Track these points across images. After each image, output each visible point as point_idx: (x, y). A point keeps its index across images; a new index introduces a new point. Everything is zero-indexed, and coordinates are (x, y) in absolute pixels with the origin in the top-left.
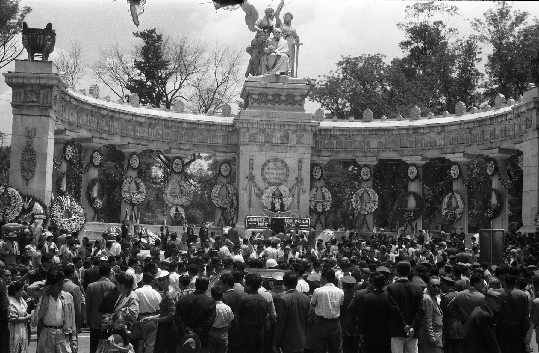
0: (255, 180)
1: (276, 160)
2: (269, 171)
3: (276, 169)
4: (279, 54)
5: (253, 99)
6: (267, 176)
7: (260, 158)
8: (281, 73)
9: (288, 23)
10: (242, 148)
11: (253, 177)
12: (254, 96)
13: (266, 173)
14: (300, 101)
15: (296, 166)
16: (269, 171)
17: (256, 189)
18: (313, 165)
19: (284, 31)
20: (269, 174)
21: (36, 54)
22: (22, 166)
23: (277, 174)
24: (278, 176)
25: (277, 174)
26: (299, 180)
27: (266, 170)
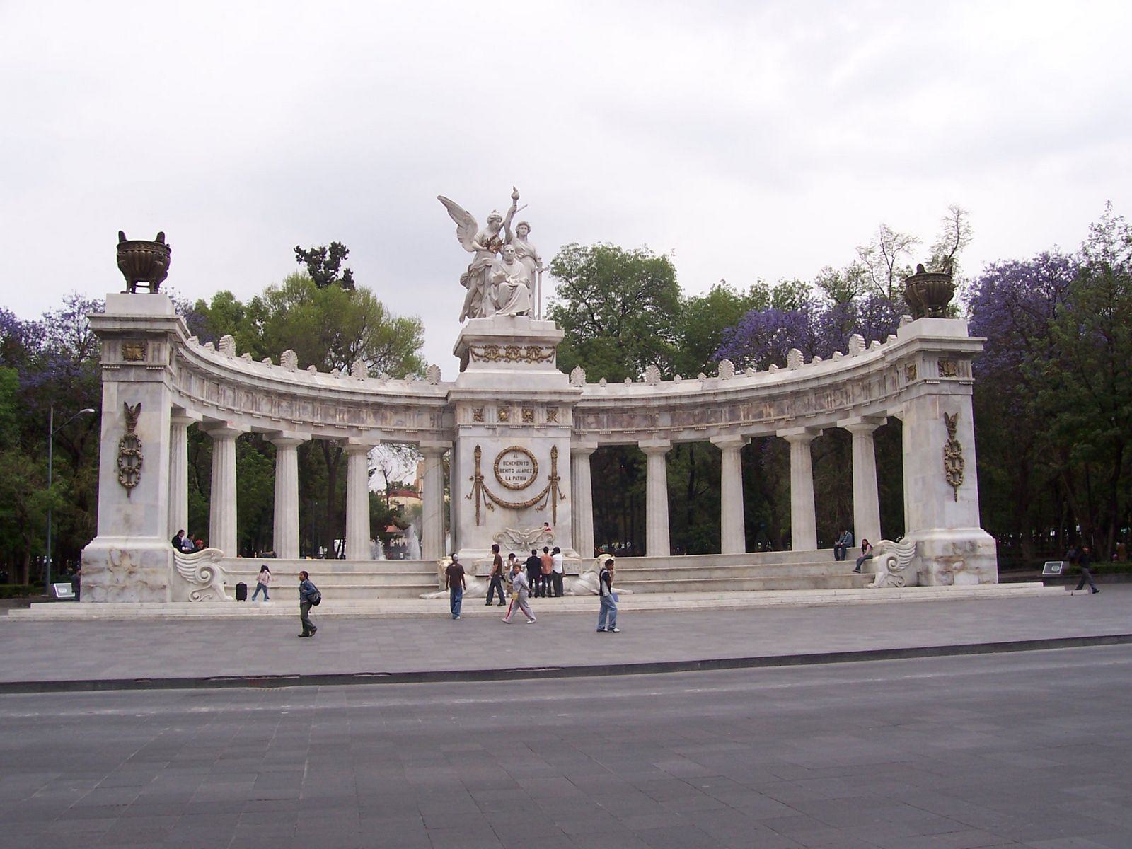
0: (484, 481)
1: (515, 450)
2: (506, 467)
4: (514, 284)
5: (477, 355)
6: (503, 476)
7: (491, 448)
8: (518, 314)
9: (522, 236)
10: (462, 433)
12: (477, 351)
13: (502, 471)
15: (548, 457)
16: (506, 467)
17: (487, 498)
18: (573, 456)
19: (518, 250)
20: (507, 471)
21: (139, 283)
22: (119, 466)
23: (518, 471)
25: (518, 471)
26: (554, 479)
27: (501, 466)
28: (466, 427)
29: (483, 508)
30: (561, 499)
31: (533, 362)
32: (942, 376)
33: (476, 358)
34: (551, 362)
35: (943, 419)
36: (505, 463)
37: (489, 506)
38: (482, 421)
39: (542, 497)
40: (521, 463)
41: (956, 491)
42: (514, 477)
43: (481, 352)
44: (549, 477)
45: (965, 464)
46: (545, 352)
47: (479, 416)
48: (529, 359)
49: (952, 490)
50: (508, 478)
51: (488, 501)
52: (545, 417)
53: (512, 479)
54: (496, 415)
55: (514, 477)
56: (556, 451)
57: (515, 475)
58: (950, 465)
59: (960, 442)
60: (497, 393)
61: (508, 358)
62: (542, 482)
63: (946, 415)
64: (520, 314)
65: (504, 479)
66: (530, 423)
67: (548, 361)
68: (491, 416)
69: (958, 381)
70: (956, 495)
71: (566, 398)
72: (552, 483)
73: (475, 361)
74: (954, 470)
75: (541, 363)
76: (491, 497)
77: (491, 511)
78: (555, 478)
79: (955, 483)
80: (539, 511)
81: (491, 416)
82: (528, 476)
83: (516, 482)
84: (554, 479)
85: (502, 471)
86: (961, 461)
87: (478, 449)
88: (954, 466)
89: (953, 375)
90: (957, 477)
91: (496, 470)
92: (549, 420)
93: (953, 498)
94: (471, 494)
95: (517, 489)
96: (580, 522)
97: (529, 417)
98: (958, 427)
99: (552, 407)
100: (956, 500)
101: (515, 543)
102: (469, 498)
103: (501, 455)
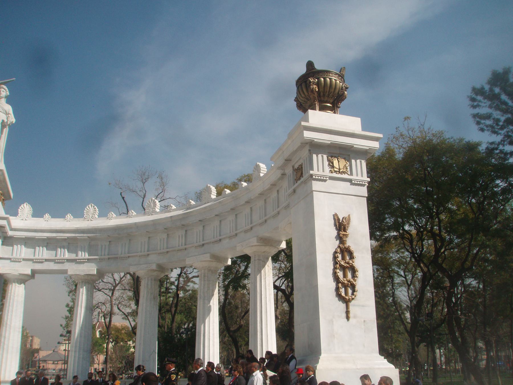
32: (332, 173)
35: (332, 222)
41: (347, 307)
45: (359, 274)
49: (343, 306)
58: (340, 274)
59: (352, 248)
63: (336, 217)
69: (350, 181)
70: (347, 312)
74: (346, 282)
79: (347, 298)
86: (354, 271)
88: (345, 276)
89: (344, 172)
90: (350, 291)
93: (344, 315)
96: (4, 343)
98: (350, 231)
100: (348, 318)
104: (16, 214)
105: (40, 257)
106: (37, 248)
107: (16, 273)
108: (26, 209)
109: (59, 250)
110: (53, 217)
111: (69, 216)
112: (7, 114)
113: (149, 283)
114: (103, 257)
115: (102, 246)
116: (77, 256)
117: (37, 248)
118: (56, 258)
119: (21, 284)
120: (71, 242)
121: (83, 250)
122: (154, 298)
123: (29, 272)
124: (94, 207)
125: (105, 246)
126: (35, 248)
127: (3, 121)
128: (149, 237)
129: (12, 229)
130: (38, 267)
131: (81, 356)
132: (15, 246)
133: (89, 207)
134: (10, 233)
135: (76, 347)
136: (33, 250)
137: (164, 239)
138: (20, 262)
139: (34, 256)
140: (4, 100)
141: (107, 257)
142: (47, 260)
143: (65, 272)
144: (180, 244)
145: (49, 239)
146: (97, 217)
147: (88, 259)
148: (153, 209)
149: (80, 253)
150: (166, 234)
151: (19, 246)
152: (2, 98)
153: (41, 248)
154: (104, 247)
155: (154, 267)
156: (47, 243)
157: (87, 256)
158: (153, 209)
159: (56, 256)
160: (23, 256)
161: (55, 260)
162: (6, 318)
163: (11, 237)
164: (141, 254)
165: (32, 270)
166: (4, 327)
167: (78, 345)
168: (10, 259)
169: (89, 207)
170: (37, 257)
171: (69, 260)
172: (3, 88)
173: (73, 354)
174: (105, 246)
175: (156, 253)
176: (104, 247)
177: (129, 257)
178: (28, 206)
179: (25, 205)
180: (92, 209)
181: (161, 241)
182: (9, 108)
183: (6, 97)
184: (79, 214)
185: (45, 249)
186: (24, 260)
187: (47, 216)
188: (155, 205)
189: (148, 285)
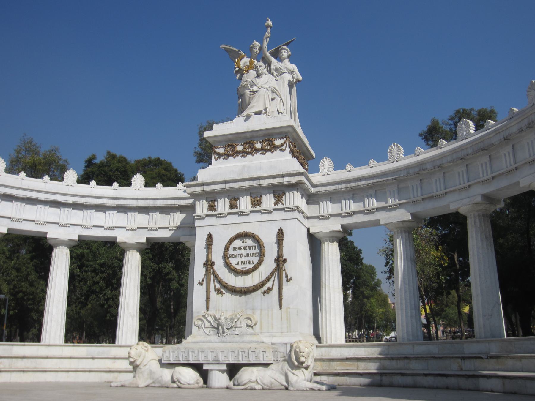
0: (215, 267)
3: (245, 248)
6: (232, 261)
8: (256, 113)
10: (197, 223)
11: (213, 264)
12: (218, 150)
13: (231, 256)
14: (282, 145)
16: (235, 252)
20: (236, 256)
23: (247, 256)
24: (249, 259)
25: (247, 256)
26: (280, 261)
27: (231, 252)
28: (202, 218)
29: (213, 294)
30: (288, 281)
31: (267, 153)
33: (217, 157)
34: (284, 151)
36: (234, 249)
37: (218, 291)
38: (215, 210)
39: (268, 279)
40: (249, 248)
42: (242, 262)
43: (221, 150)
44: (275, 259)
46: (278, 142)
47: (212, 208)
48: (264, 151)
50: (236, 263)
51: (218, 286)
52: (273, 201)
53: (240, 263)
54: (228, 204)
55: (242, 262)
56: (282, 233)
57: (244, 260)
60: (226, 182)
61: (245, 153)
62: (269, 265)
64: (258, 113)
65: (233, 264)
66: (258, 208)
67: (281, 150)
68: (223, 205)
71: (286, 180)
72: (278, 265)
73: (216, 160)
75: (275, 152)
76: (220, 282)
77: (220, 295)
78: (281, 259)
80: (265, 294)
81: (223, 205)
82: (256, 260)
83: (243, 266)
84: (280, 261)
85: (231, 256)
87: (210, 238)
91: (225, 257)
92: (276, 204)
94: (203, 281)
95: (247, 273)
97: (256, 203)
99: (279, 191)
101: (214, 327)
102: (201, 284)
103: (231, 241)
104: (317, 171)
105: (348, 210)
106: (344, 202)
107: (326, 231)
108: (326, 164)
109: (366, 200)
110: (355, 166)
111: (372, 162)
112: (292, 72)
113: (477, 220)
114: (415, 199)
115: (413, 186)
116: (387, 203)
117: (344, 202)
118: (365, 209)
119: (333, 242)
120: (375, 187)
121: (392, 196)
122: (486, 238)
123: (339, 228)
124: (397, 145)
125: (416, 185)
126: (341, 203)
127: (289, 81)
128: (467, 165)
129: (314, 186)
130: (347, 221)
131: (409, 314)
132: (321, 204)
133: (392, 147)
134: (313, 190)
135: (401, 304)
136: (340, 204)
137: (486, 163)
138: (328, 218)
139: (342, 210)
140: (287, 62)
141: (420, 198)
142: (355, 213)
143: (376, 223)
144: (509, 165)
145: (352, 189)
146: (403, 156)
147: (400, 204)
148: (466, 131)
149: (389, 200)
150: (488, 156)
151: (325, 202)
152: (285, 59)
153: (347, 201)
154: (415, 187)
155: (479, 199)
156: (353, 194)
157: (397, 202)
158: (466, 131)
159: (364, 207)
160: (330, 212)
161: (364, 211)
162: (323, 279)
163: (316, 195)
164: (461, 186)
165: (342, 226)
166: (324, 289)
167: (404, 302)
168: (318, 217)
169: (392, 147)
170: (344, 210)
171: (378, 209)
172: (284, 49)
173: (400, 312)
174: (416, 185)
175: (479, 182)
176: (415, 187)
177: (446, 193)
178: (328, 161)
179: (325, 159)
180: (395, 149)
181: (482, 165)
182: (293, 67)
183: (289, 57)
184: (382, 158)
185: (351, 201)
186: (332, 216)
187: (349, 167)
188: (468, 126)
189: (475, 222)
